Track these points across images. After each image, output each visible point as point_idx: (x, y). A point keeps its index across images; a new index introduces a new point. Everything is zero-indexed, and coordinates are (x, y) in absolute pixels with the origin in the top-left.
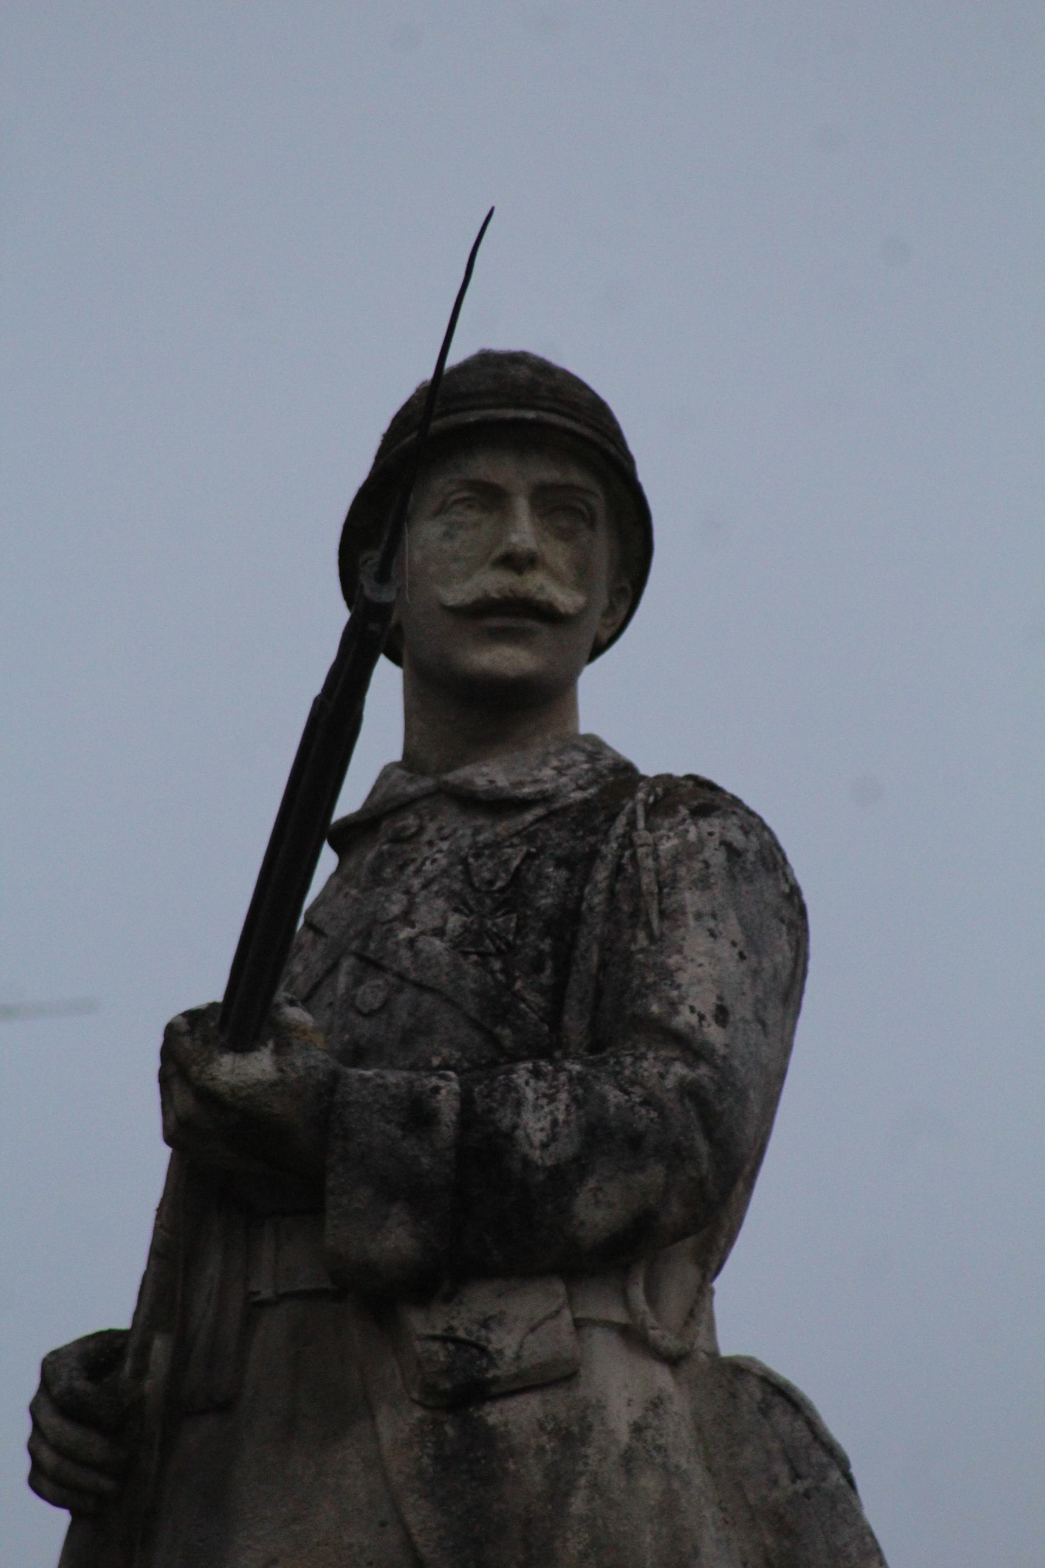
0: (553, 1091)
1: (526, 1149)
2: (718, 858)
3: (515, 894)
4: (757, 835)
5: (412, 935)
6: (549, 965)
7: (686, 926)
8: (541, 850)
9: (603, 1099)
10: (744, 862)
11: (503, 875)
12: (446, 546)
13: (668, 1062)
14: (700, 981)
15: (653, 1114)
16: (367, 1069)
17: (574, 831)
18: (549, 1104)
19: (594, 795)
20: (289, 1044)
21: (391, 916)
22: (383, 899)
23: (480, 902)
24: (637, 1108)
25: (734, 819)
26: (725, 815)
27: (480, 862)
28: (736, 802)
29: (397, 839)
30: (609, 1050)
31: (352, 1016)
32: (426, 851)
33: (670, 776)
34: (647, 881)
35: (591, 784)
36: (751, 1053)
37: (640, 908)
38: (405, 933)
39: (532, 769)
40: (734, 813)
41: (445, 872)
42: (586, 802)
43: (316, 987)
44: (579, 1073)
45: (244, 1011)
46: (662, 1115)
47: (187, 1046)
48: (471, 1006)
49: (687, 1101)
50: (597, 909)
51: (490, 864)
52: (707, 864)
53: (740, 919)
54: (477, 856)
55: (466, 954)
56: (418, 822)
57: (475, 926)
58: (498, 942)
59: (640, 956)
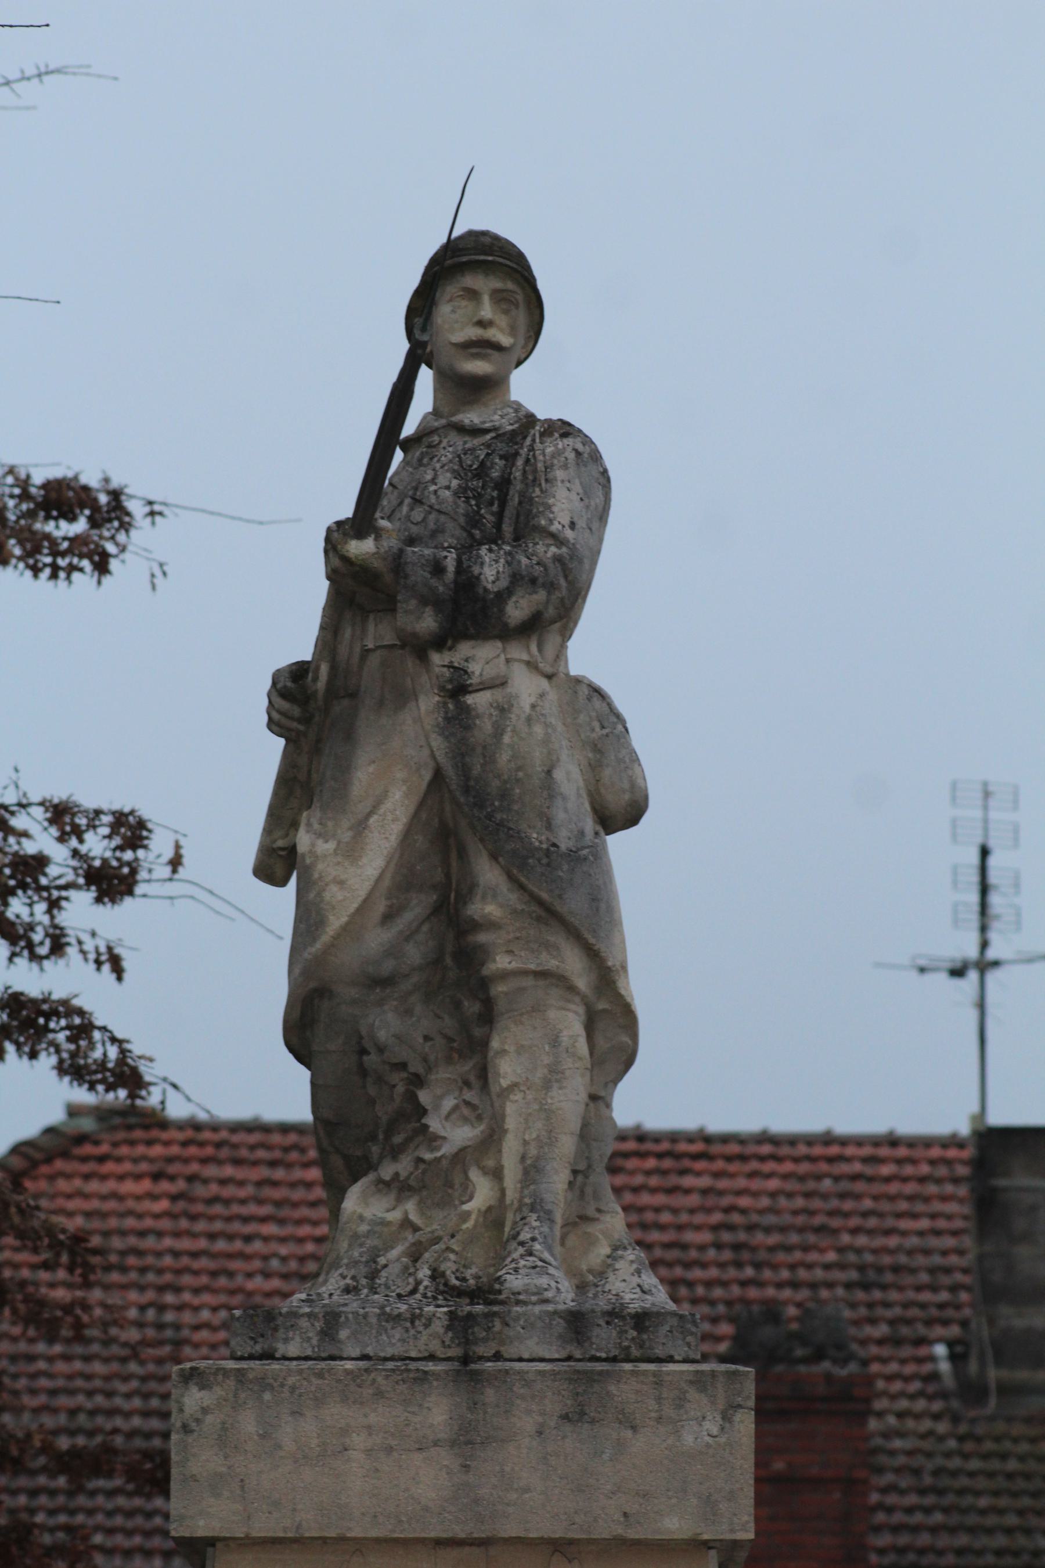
1: (485, 584)
2: (571, 456)
3: (482, 471)
8: (493, 451)
9: (519, 562)
12: (452, 316)
13: (548, 546)
14: (563, 510)
23: (466, 474)
25: (579, 439)
26: (575, 437)
28: (580, 431)
29: (430, 446)
32: (442, 452)
34: (540, 466)
35: (516, 422)
37: (537, 477)
38: (433, 488)
41: (451, 461)
43: (393, 511)
45: (361, 523)
46: (546, 569)
47: (336, 537)
48: (462, 520)
52: (566, 459)
53: (581, 483)
54: (465, 454)
55: (459, 497)
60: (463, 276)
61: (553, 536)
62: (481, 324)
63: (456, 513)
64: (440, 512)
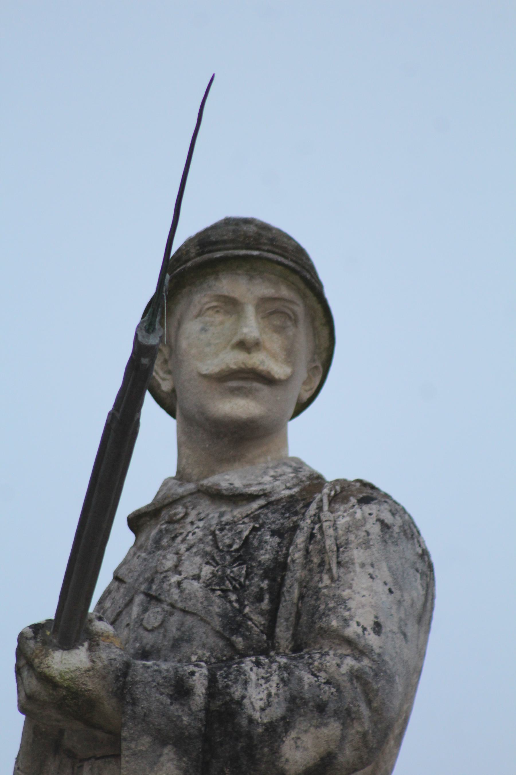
0: (269, 675)
1: (250, 711)
2: (375, 529)
3: (245, 553)
4: (400, 516)
5: (180, 579)
6: (267, 597)
7: (354, 571)
8: (262, 526)
9: (300, 680)
10: (392, 532)
11: (238, 541)
12: (203, 336)
13: (342, 657)
14: (363, 606)
15: (333, 690)
16: (147, 660)
17: (283, 514)
18: (266, 683)
19: (297, 493)
20: (98, 645)
21: (166, 568)
22: (161, 558)
23: (223, 558)
24: (322, 686)
25: (386, 506)
26: (380, 503)
27: (223, 533)
28: (387, 496)
29: (171, 522)
30: (305, 650)
31: (141, 631)
32: (189, 528)
33: (345, 481)
34: (330, 543)
35: (295, 486)
36: (396, 653)
37: (324, 559)
38: (175, 579)
39: (257, 477)
40: (386, 502)
41: (201, 540)
42: (291, 496)
43: (119, 614)
44: (286, 663)
45: (69, 624)
46: (339, 690)
47: (32, 647)
48: (217, 623)
49: (355, 681)
50: (297, 561)
51: (230, 534)
52: (368, 534)
53: (390, 568)
54: (221, 530)
55: (213, 590)
56: (184, 510)
57: (220, 573)
58: (234, 583)
59: (325, 591)
60: (217, 279)
61: (349, 642)
62: (243, 345)
63: (208, 612)
64: (184, 611)
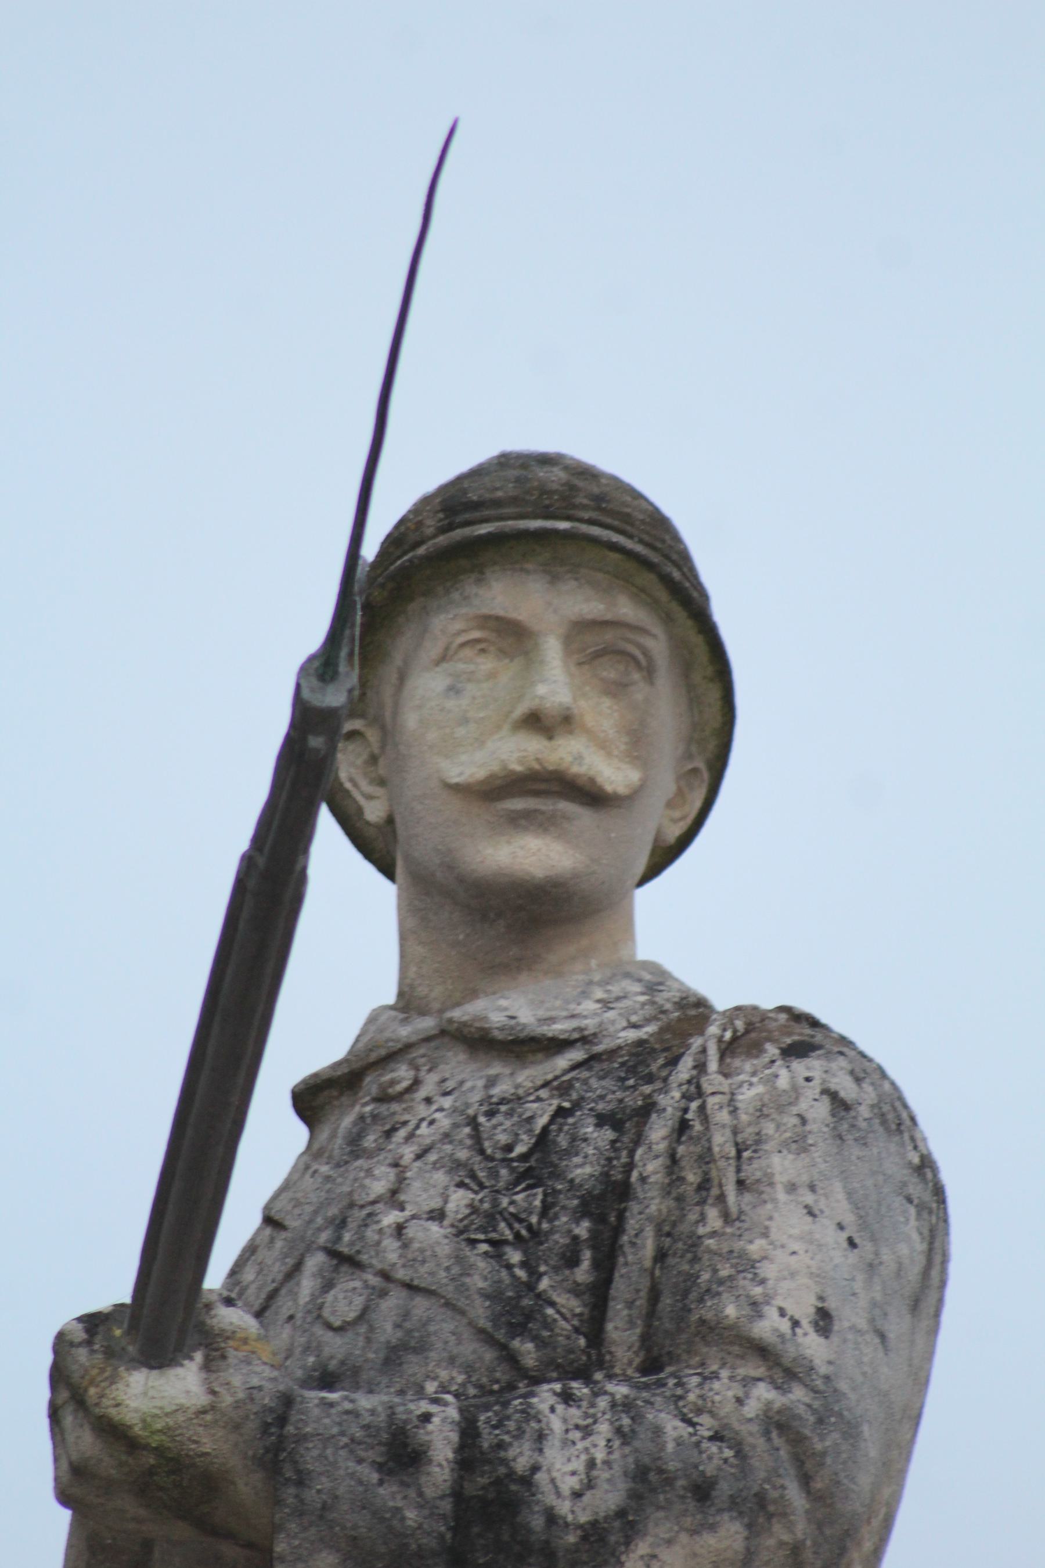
1: (551, 1499)
2: (820, 1111)
3: (539, 1164)
8: (577, 1105)
9: (658, 1431)
12: (450, 704)
13: (748, 1382)
23: (494, 1174)
26: (829, 1056)
32: (422, 1110)
34: (721, 1141)
38: (391, 1218)
41: (447, 1137)
43: (272, 1295)
45: (164, 1312)
46: (739, 1453)
48: (480, 1311)
52: (804, 1121)
53: (850, 1194)
55: (473, 1242)
61: (762, 1351)
62: (535, 722)
63: (462, 1289)
64: (410, 1287)
